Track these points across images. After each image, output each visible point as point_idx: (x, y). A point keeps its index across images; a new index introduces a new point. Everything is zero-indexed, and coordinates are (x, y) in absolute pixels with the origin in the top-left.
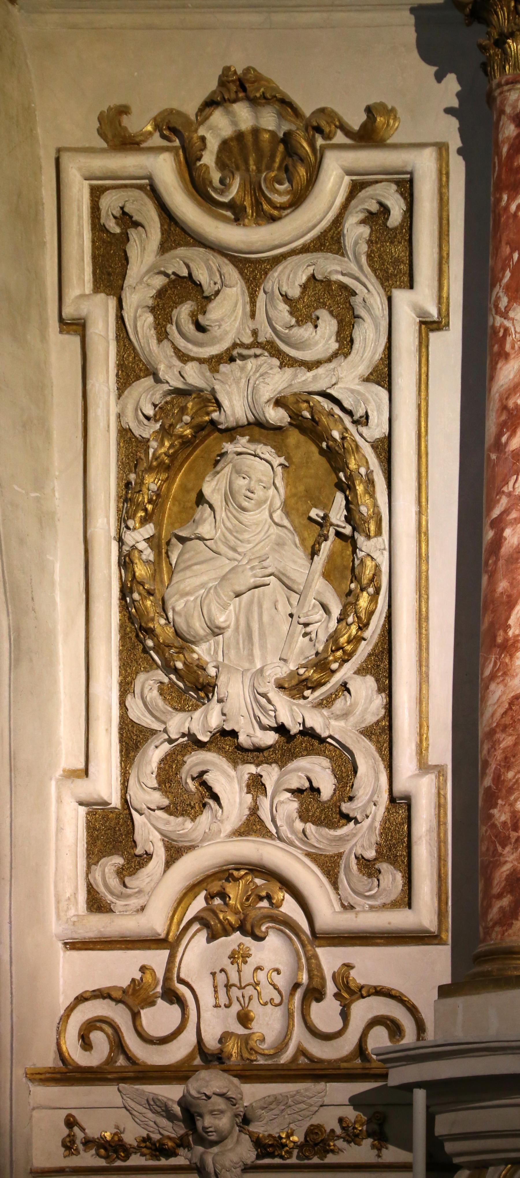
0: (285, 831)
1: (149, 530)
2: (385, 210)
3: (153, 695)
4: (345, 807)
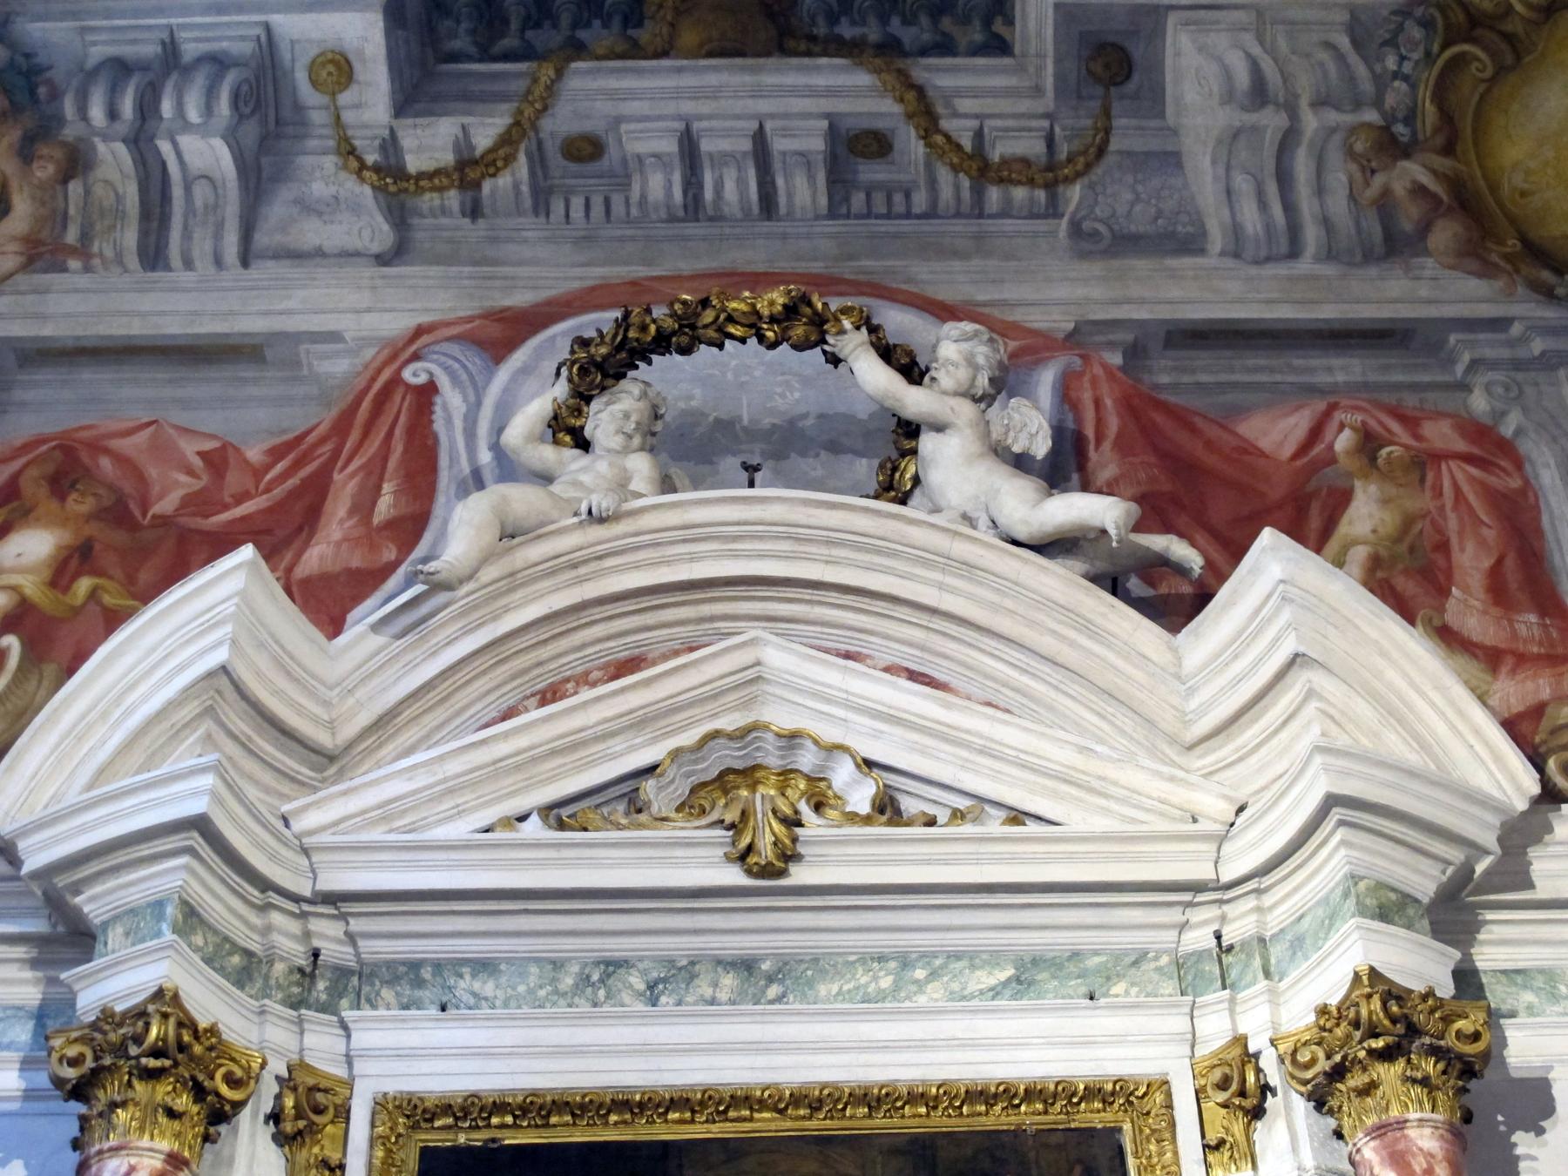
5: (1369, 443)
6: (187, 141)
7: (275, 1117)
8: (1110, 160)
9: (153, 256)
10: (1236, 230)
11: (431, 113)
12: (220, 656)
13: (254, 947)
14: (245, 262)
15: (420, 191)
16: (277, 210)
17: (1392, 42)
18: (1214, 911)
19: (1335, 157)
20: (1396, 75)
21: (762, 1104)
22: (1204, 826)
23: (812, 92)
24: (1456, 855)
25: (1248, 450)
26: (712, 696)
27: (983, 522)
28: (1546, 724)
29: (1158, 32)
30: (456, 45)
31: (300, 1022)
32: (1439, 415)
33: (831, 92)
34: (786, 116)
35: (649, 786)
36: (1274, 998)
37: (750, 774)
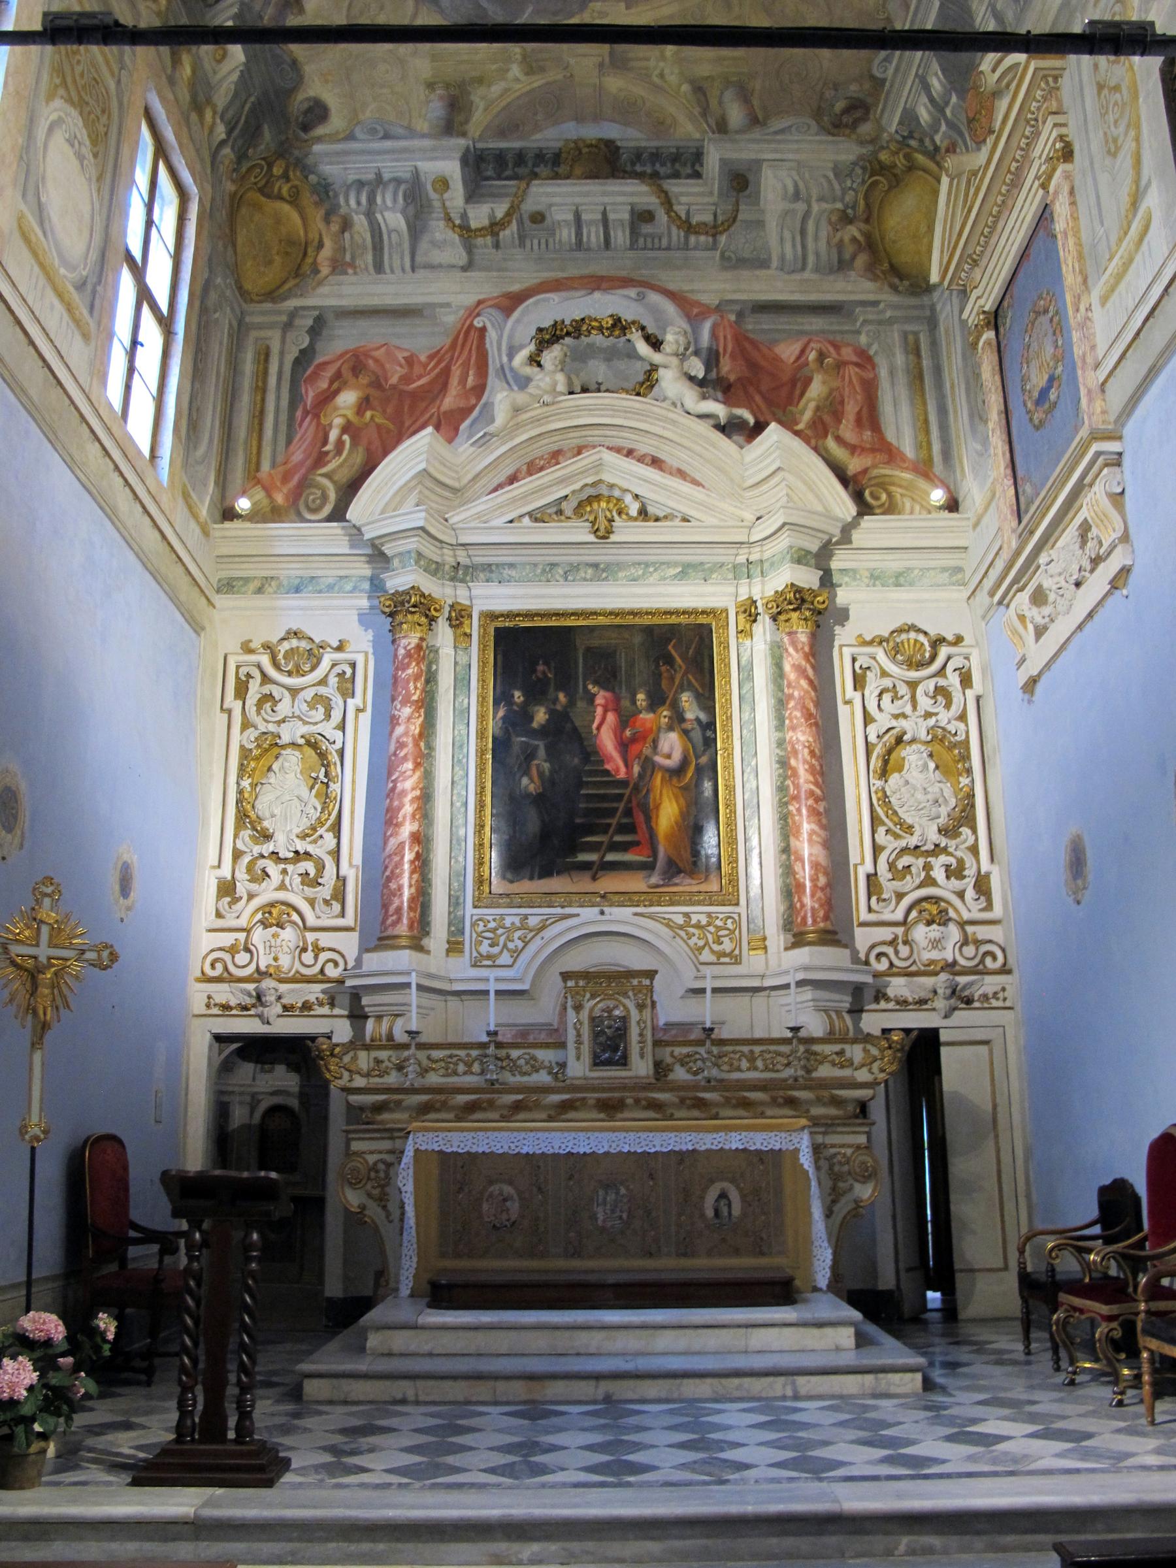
0: (295, 889)
1: (250, 780)
2: (344, 673)
3: (247, 839)
4: (320, 880)
5: (821, 356)
6: (386, 214)
7: (449, 619)
8: (737, 224)
9: (379, 267)
10: (782, 258)
11: (478, 202)
12: (423, 466)
13: (439, 560)
14: (413, 270)
15: (476, 237)
16: (423, 245)
17: (850, 175)
18: (746, 551)
19: (824, 224)
20: (851, 188)
21: (600, 614)
22: (745, 524)
23: (624, 194)
24: (826, 537)
25: (777, 359)
26: (584, 472)
27: (679, 405)
28: (867, 476)
29: (759, 170)
30: (490, 173)
31: (455, 587)
32: (848, 345)
33: (632, 194)
34: (614, 204)
35: (564, 505)
36: (763, 584)
37: (598, 498)
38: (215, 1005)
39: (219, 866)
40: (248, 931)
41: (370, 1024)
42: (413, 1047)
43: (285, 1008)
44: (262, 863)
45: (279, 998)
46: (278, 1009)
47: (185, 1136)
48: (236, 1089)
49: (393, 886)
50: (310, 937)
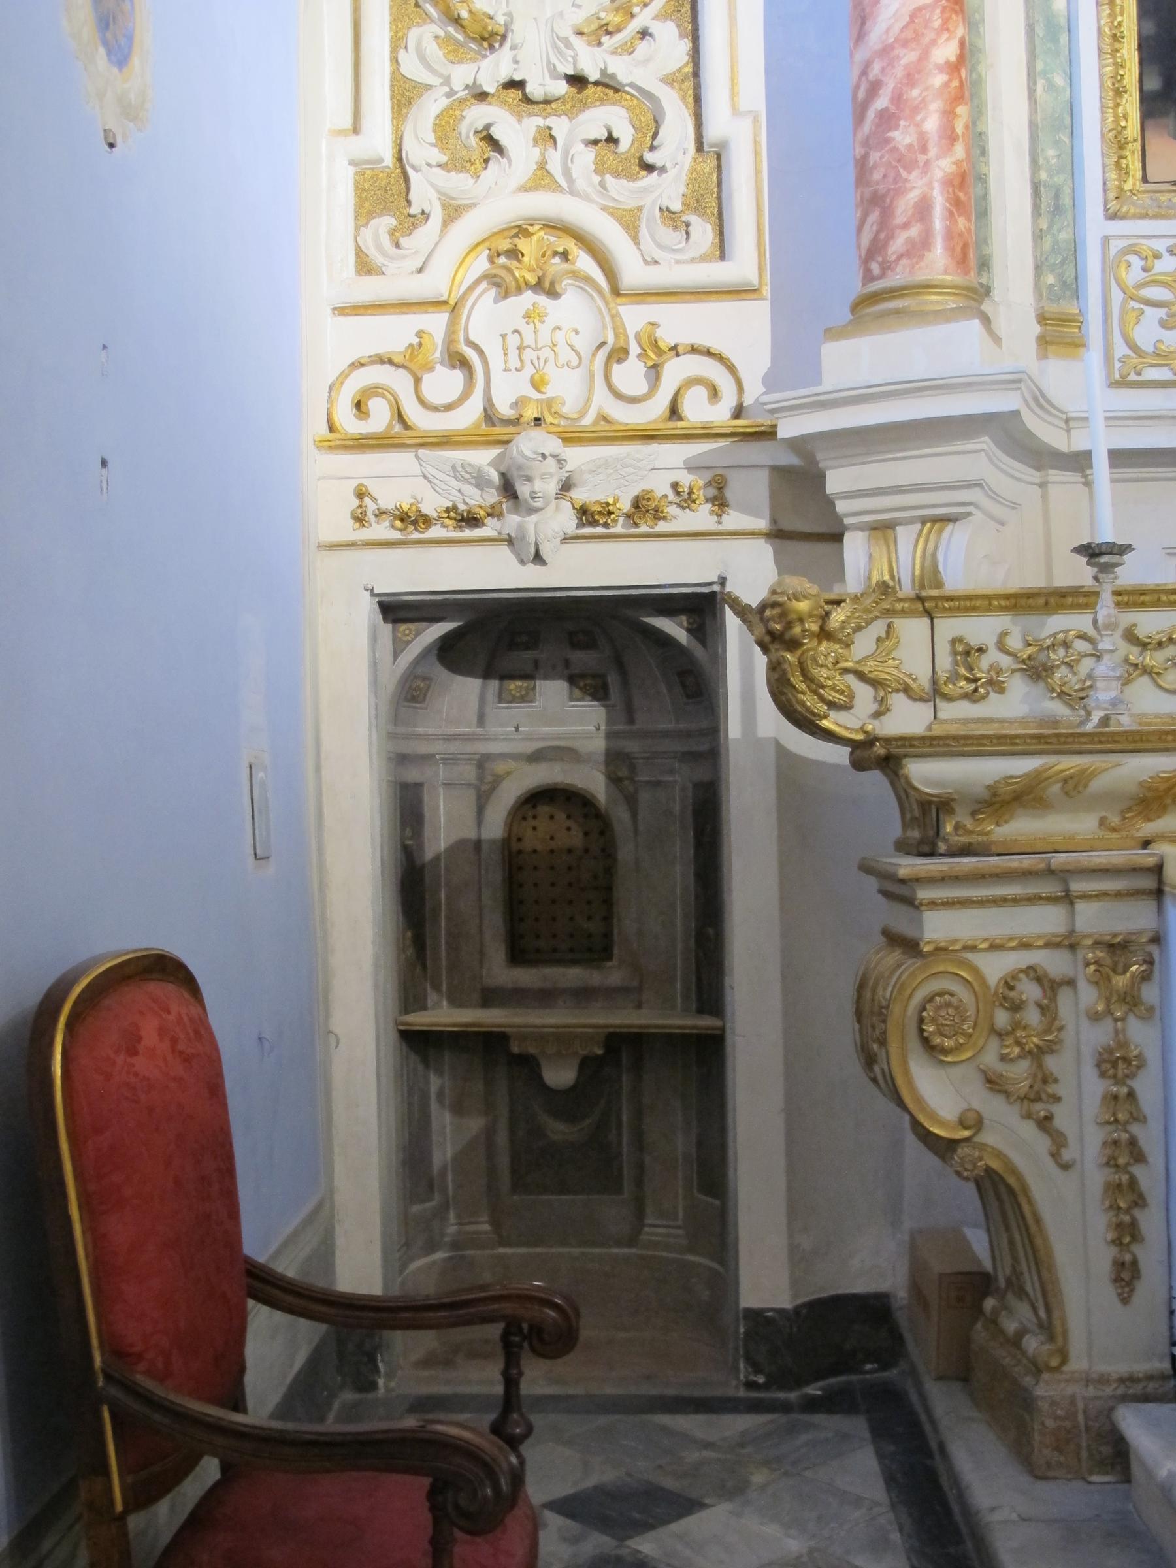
0: (581, 184)
3: (433, 50)
4: (650, 158)
38: (380, 514)
39: (356, 130)
40: (452, 307)
41: (855, 547)
42: (1107, 598)
43: (585, 515)
44: (478, 115)
45: (566, 486)
46: (566, 519)
47: (323, 887)
48: (437, 748)
49: (903, 137)
50: (634, 317)
